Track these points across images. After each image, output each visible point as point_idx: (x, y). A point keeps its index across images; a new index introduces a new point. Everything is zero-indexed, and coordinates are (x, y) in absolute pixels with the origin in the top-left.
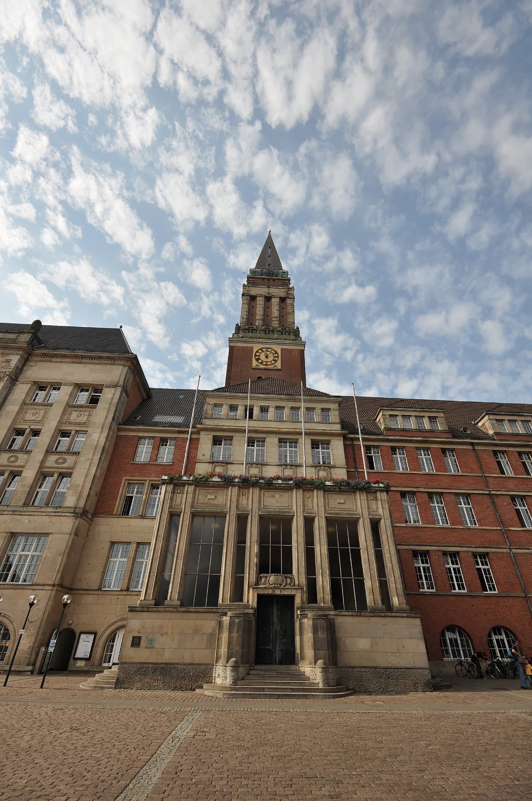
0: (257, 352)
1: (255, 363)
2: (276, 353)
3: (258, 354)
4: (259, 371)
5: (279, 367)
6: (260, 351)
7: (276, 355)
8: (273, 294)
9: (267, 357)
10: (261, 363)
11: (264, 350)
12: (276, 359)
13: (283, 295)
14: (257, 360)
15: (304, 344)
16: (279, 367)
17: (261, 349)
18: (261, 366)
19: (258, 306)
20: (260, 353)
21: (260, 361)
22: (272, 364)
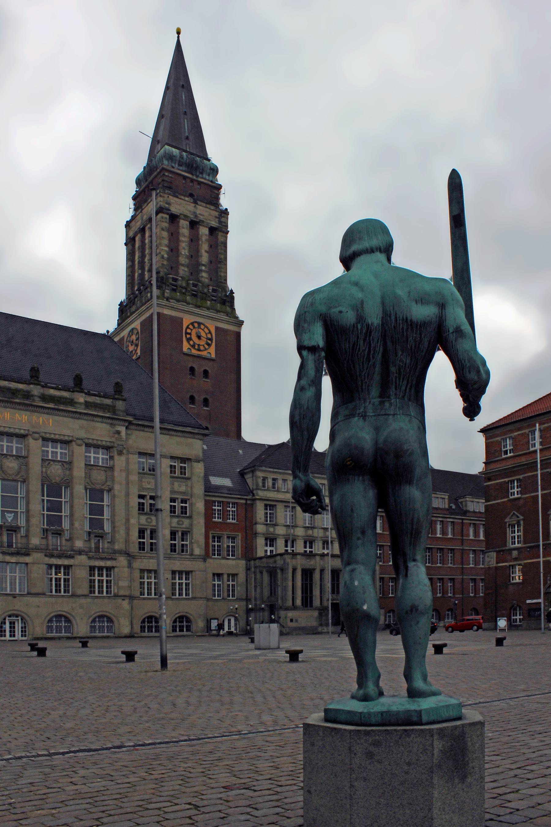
0: (188, 327)
1: (186, 346)
2: (210, 332)
3: (189, 331)
4: (191, 359)
5: (213, 356)
6: (191, 327)
7: (209, 336)
8: (201, 218)
9: (199, 337)
10: (193, 346)
11: (196, 325)
12: (210, 342)
13: (214, 224)
14: (189, 340)
15: (240, 323)
16: (213, 356)
17: (192, 324)
18: (194, 352)
19: (182, 238)
20: (192, 330)
21: (191, 343)
22: (206, 349)
